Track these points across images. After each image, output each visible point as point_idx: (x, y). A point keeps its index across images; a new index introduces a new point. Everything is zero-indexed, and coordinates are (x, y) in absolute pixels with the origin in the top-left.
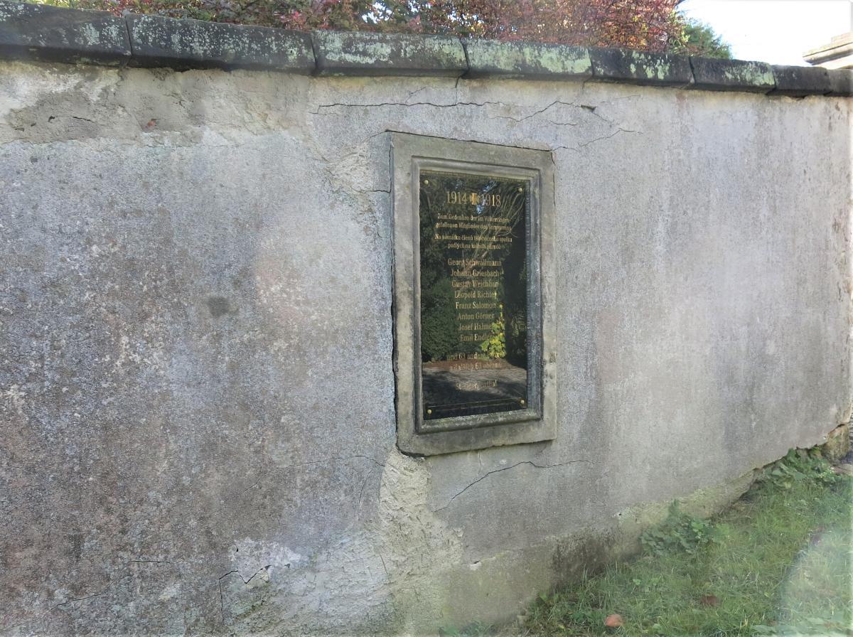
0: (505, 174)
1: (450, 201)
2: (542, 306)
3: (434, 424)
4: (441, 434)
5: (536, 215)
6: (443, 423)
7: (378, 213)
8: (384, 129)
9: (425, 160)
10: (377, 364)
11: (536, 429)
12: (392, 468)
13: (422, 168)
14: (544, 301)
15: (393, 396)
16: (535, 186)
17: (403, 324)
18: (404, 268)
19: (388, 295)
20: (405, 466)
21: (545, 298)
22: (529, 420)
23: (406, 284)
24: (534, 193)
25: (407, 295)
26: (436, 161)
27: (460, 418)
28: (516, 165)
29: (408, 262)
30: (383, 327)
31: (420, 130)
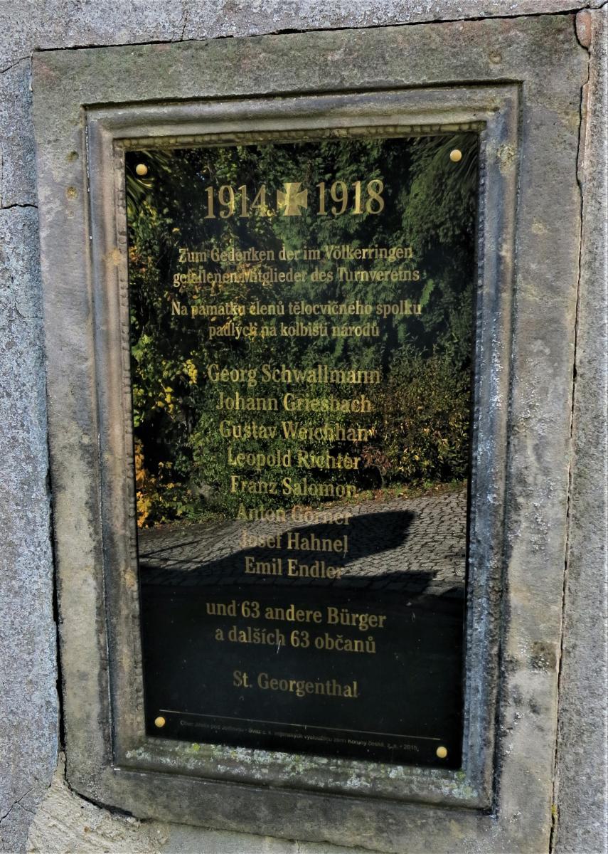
0: (386, 115)
1: (216, 212)
2: (510, 504)
3: (162, 754)
4: (176, 782)
5: (501, 228)
6: (190, 754)
7: (13, 262)
8: (27, 49)
9: (121, 112)
10: (17, 600)
11: (472, 835)
12: (55, 822)
13: (119, 134)
14: (518, 489)
15: (55, 675)
16: (505, 133)
17: (72, 520)
18: (67, 389)
19: (39, 449)
20: (87, 824)
21: (522, 481)
22: (450, 807)
23: (74, 427)
24: (498, 160)
25: (79, 453)
26: (152, 110)
27: (241, 753)
28: (424, 79)
29: (81, 374)
30: (28, 522)
31: (124, 31)
